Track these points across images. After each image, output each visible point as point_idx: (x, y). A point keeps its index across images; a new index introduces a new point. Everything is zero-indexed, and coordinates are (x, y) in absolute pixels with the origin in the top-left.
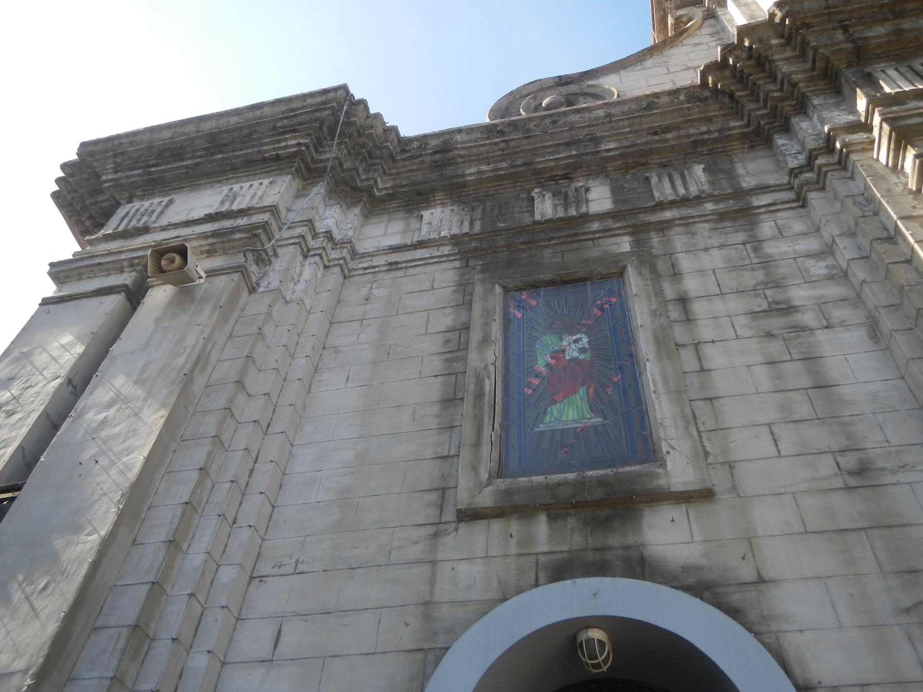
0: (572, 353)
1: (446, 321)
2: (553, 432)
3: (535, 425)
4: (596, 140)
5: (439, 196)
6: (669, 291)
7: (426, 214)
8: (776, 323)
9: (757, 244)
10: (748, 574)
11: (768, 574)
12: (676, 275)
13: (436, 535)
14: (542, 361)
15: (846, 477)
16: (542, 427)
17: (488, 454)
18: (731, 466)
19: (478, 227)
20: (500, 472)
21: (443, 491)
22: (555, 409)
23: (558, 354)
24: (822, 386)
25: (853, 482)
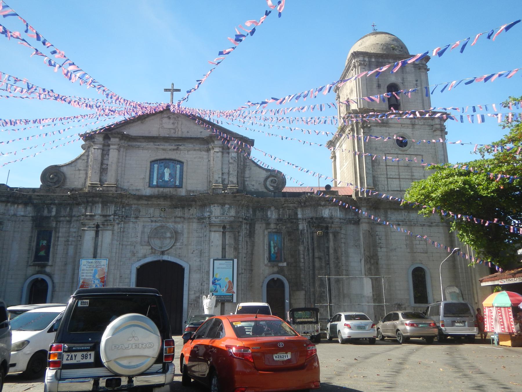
0: (44, 244)
1: (29, 235)
4: (55, 200)
5: (30, 204)
6: (57, 236)
7: (28, 208)
8: (67, 243)
9: (69, 228)
10: (53, 273)
12: (59, 232)
13: (27, 267)
14: (41, 245)
17: (33, 258)
18: (55, 262)
19: (36, 214)
20: (34, 261)
21: (28, 262)
22: (41, 252)
23: (43, 244)
24: (67, 253)
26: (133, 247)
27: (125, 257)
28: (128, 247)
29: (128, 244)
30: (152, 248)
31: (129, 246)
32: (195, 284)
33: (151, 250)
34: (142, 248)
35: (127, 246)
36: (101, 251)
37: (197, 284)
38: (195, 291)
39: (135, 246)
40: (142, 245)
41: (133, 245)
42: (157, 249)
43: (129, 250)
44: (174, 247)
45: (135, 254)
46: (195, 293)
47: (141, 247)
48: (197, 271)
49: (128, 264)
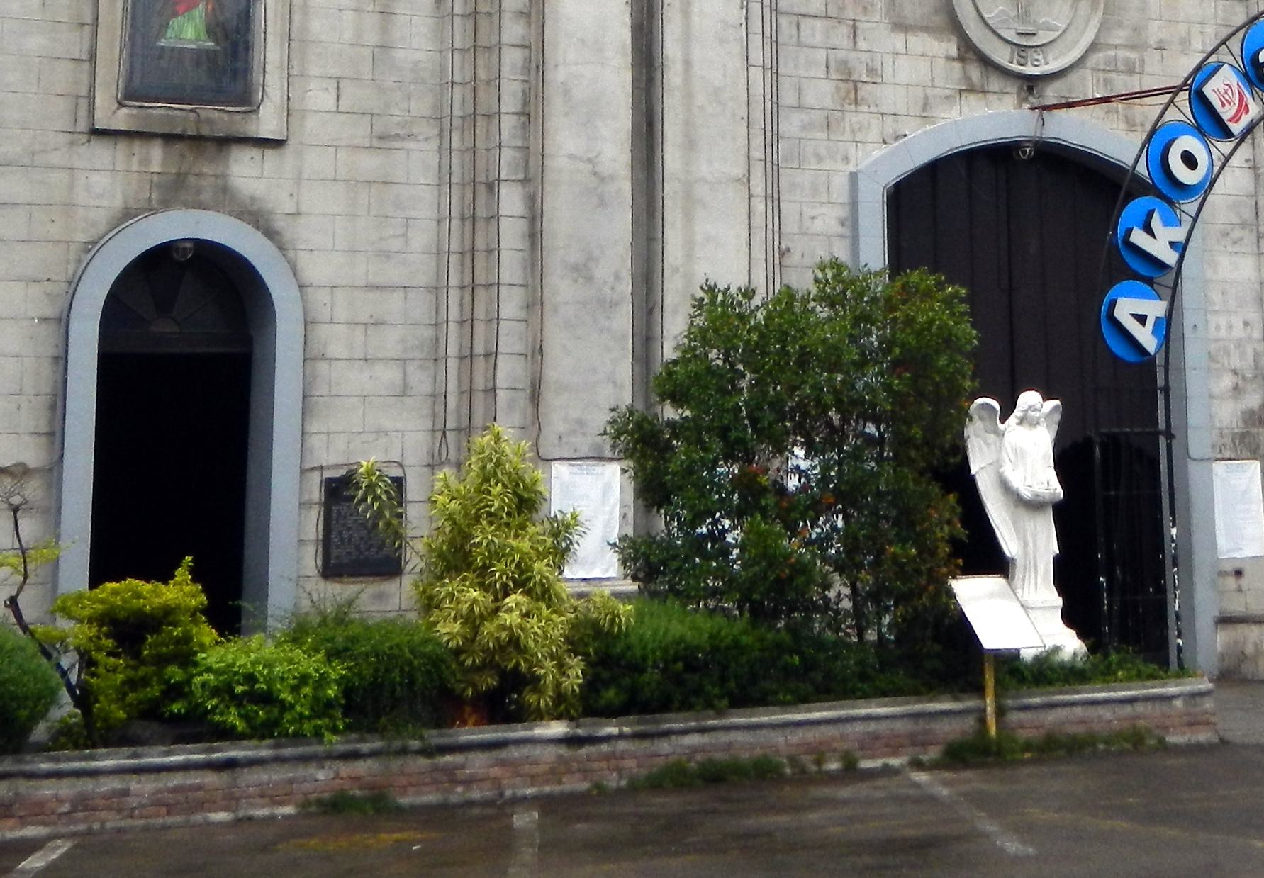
2: (173, 49)
3: (158, 38)
11: (303, 209)
15: (374, 140)
16: (163, 43)
22: (175, 23)
25: (376, 143)
26: (841, 36)
27: (800, 107)
28: (814, 31)
29: (813, 11)
30: (969, 52)
31: (818, 24)
32: (1230, 327)
33: (957, 66)
34: (900, 46)
35: (805, 24)
36: (687, 38)
37: (1246, 324)
38: (1235, 372)
39: (855, 29)
40: (900, 26)
41: (839, 20)
42: (1002, 56)
43: (821, 55)
44: (1097, 58)
45: (864, 91)
46: (1236, 388)
47: (898, 41)
48: (1237, 233)
49: (820, 159)
